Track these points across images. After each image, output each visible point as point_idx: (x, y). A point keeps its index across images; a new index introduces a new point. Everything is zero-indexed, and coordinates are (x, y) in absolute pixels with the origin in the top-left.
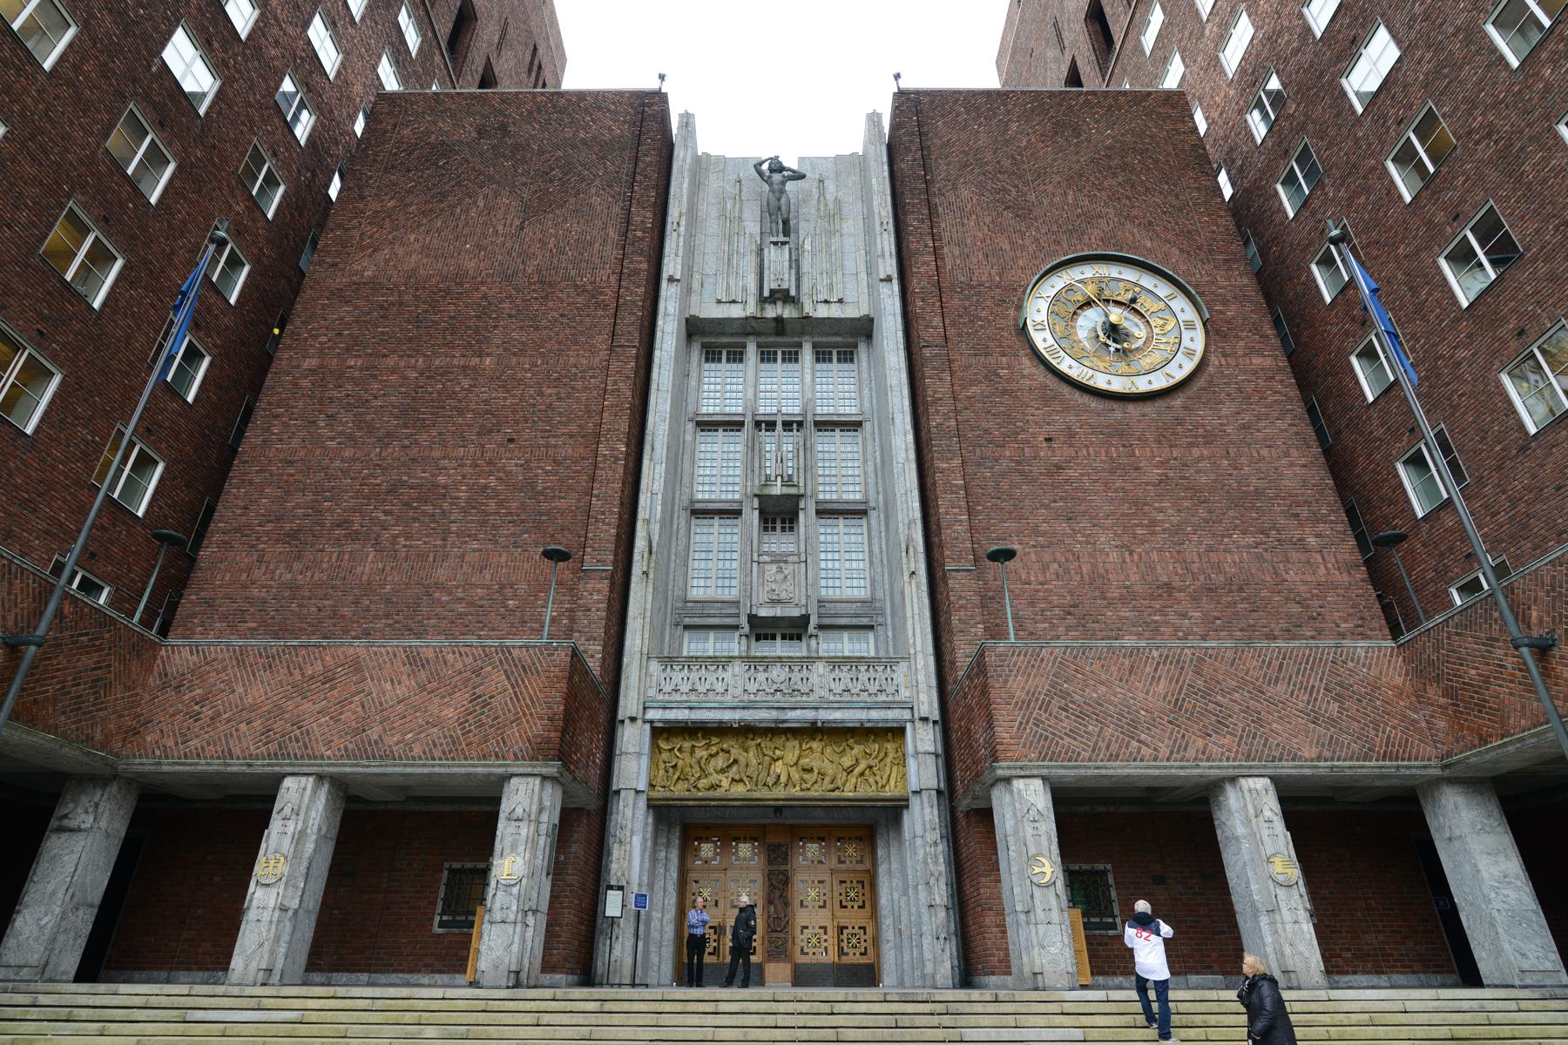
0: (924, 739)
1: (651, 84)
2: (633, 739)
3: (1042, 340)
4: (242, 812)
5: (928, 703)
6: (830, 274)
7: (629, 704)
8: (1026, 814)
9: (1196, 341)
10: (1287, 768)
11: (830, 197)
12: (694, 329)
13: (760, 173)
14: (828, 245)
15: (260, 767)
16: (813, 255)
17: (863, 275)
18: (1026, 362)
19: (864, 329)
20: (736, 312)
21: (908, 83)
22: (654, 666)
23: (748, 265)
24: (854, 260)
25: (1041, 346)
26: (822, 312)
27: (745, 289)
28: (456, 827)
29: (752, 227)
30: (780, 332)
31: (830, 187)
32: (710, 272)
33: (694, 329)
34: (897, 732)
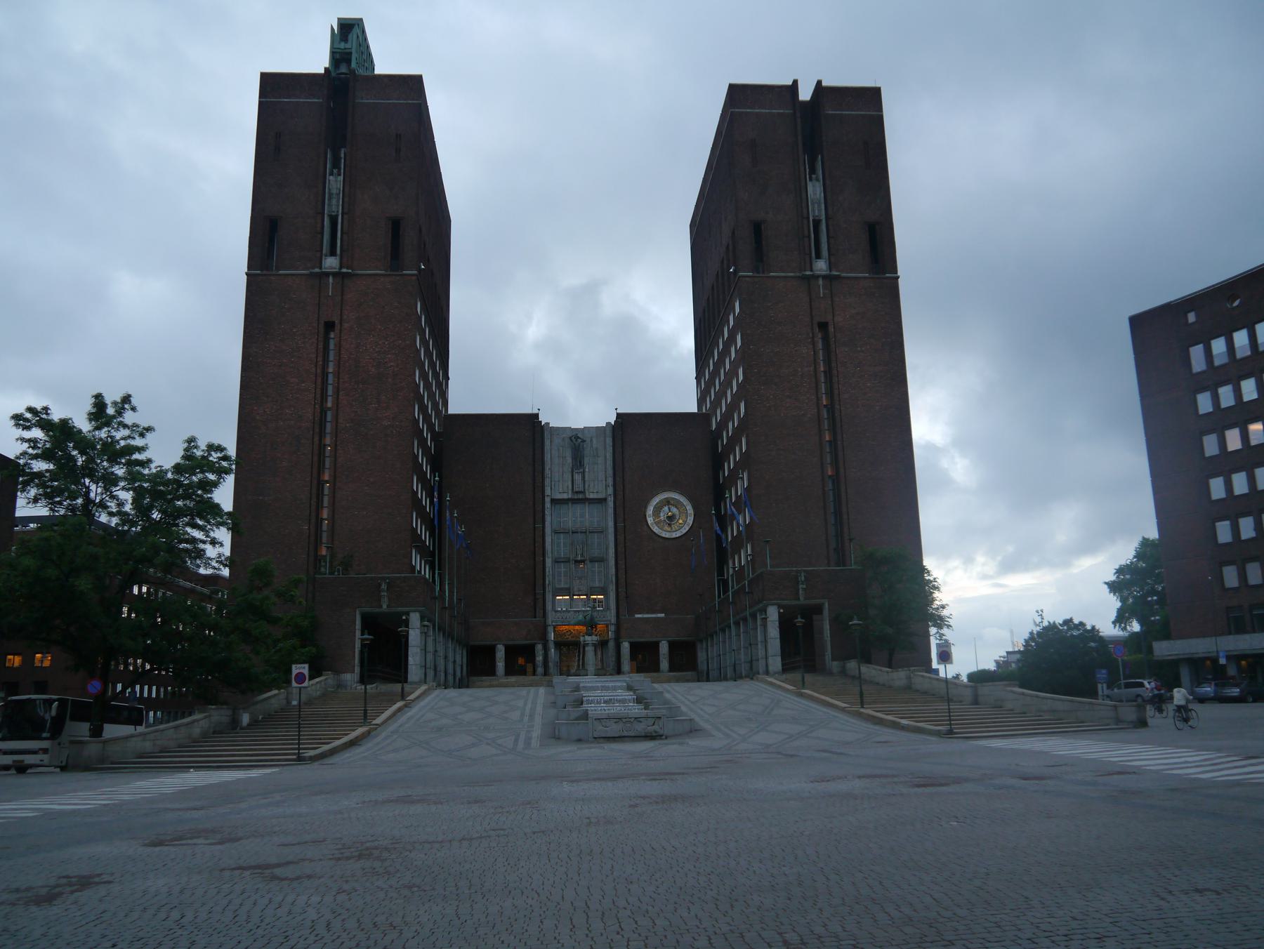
2: (550, 629)
3: (650, 520)
4: (491, 650)
5: (613, 620)
7: (549, 621)
8: (626, 646)
9: (690, 520)
19: (605, 500)
20: (565, 496)
23: (568, 476)
26: (592, 496)
28: (528, 651)
29: (569, 460)
30: (579, 499)
32: (558, 482)
33: (554, 501)
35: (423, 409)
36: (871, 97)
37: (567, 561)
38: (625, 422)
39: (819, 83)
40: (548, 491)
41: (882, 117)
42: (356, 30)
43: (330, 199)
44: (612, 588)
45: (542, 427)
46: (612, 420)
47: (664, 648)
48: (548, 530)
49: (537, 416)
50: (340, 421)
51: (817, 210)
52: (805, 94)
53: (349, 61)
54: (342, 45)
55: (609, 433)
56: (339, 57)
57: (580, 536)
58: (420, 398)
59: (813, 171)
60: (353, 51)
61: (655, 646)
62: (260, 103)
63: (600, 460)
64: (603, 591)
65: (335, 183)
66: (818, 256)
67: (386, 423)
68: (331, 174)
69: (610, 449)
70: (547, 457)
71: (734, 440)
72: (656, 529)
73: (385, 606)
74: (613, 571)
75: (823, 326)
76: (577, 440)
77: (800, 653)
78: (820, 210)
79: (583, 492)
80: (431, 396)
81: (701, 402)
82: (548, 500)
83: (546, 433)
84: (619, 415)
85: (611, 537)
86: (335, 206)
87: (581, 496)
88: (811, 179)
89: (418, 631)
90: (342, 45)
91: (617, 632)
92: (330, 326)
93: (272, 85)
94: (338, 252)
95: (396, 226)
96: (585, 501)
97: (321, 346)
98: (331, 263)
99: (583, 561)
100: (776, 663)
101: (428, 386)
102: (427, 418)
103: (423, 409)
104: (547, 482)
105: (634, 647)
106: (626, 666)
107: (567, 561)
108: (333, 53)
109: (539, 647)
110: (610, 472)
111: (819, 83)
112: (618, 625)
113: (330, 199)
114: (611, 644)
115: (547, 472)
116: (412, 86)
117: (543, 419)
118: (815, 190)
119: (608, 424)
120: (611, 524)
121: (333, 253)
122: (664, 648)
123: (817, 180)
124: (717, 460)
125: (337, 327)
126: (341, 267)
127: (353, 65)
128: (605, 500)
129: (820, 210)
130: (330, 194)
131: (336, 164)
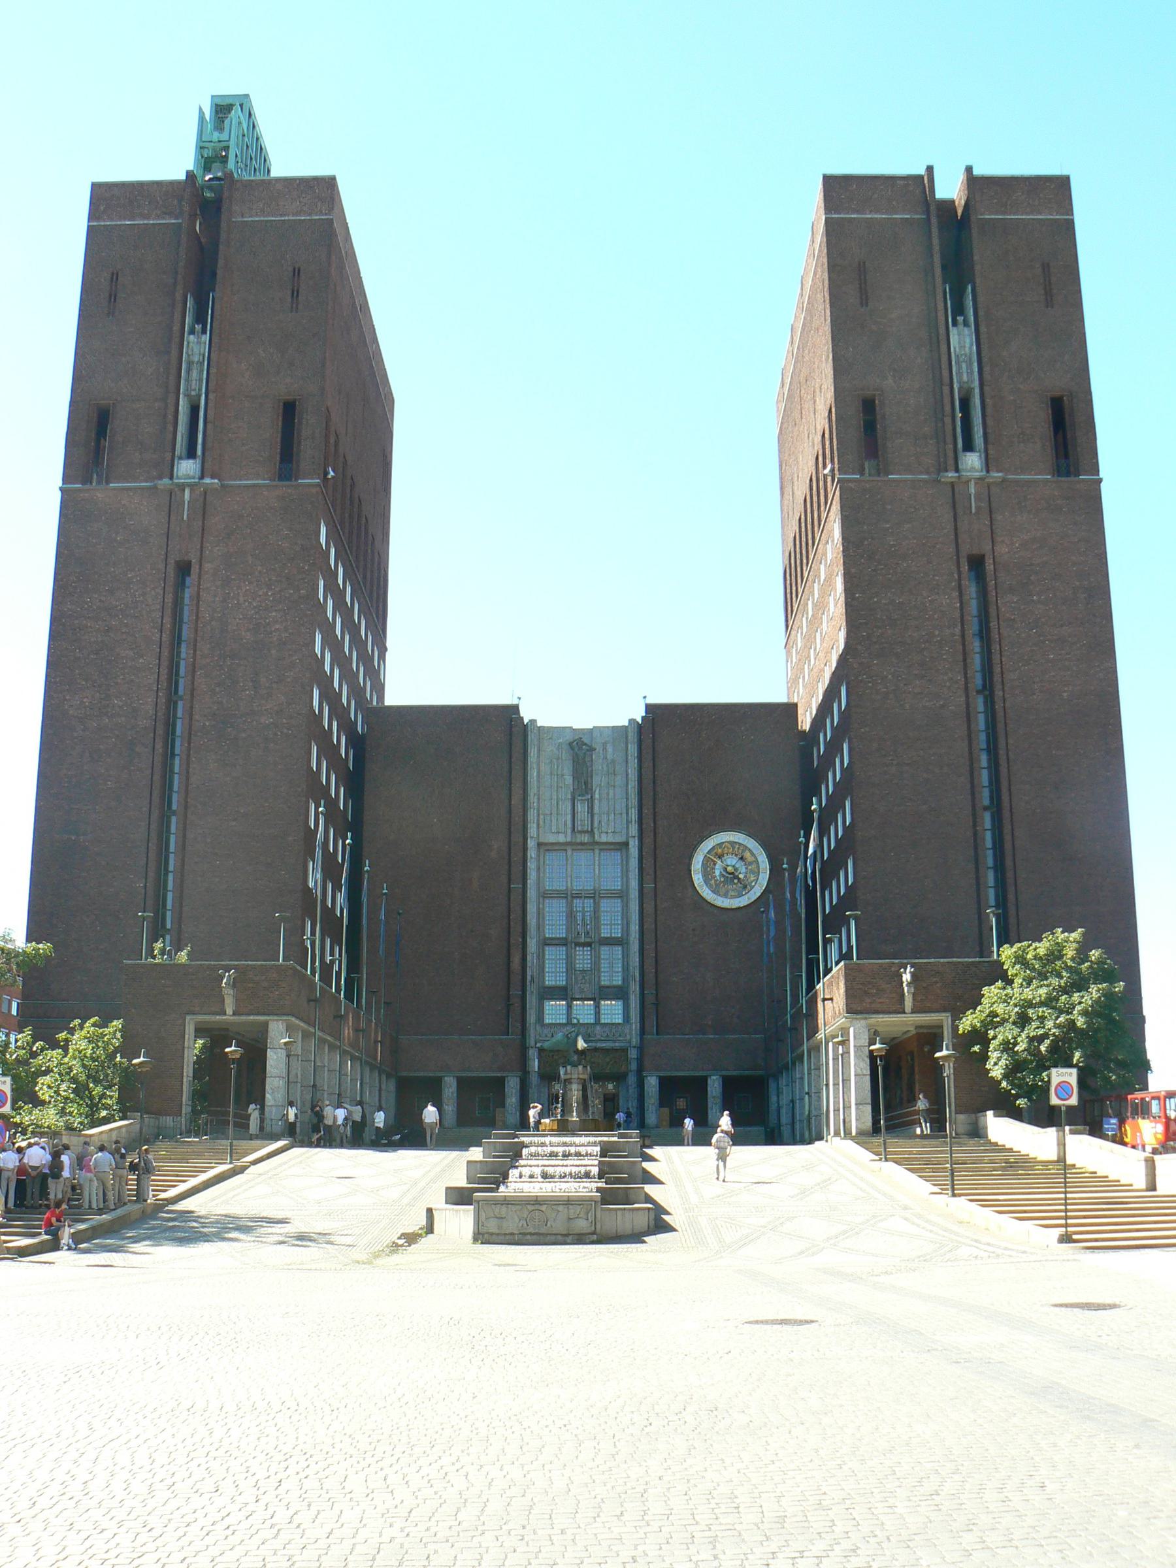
0: (633, 1054)
1: (515, 702)
2: (533, 1054)
3: (697, 879)
5: (635, 1041)
6: (608, 814)
7: (531, 1041)
8: (652, 1083)
10: (724, 1073)
11: (609, 757)
12: (539, 845)
13: (572, 749)
14: (608, 794)
15: (439, 1074)
16: (600, 800)
17: (624, 815)
18: (690, 890)
21: (650, 701)
22: (538, 1028)
24: (620, 806)
25: (696, 883)
26: (604, 839)
27: (565, 824)
29: (569, 780)
31: (610, 749)
34: (624, 1050)
35: (331, 697)
36: (1056, 190)
37: (563, 942)
38: (658, 715)
39: (969, 169)
40: (532, 830)
41: (1069, 228)
42: (235, 113)
43: (189, 370)
44: (634, 989)
45: (525, 726)
46: (639, 714)
47: (714, 1086)
48: (531, 894)
49: (515, 709)
50: (196, 717)
51: (966, 374)
52: (950, 188)
53: (225, 160)
54: (216, 136)
55: (632, 736)
56: (211, 156)
57: (588, 904)
58: (325, 683)
59: (959, 310)
60: (232, 144)
61: (700, 1084)
62: (91, 231)
63: (619, 780)
64: (619, 993)
65: (196, 345)
66: (969, 447)
67: (266, 720)
68: (192, 332)
69: (633, 763)
70: (533, 775)
71: (834, 747)
72: (706, 893)
73: (229, 1011)
74: (635, 960)
75: (977, 563)
76: (580, 748)
77: (914, 1098)
78: (970, 373)
79: (591, 832)
80: (349, 676)
81: (792, 684)
82: (531, 844)
83: (531, 738)
84: (649, 708)
85: (634, 906)
86: (194, 381)
87: (586, 838)
88: (955, 324)
89: (282, 1054)
90: (216, 136)
91: (640, 1060)
92: (184, 569)
93: (107, 200)
94: (199, 452)
95: (289, 410)
96: (592, 845)
97: (169, 598)
98: (187, 468)
99: (589, 944)
100: (858, 1116)
101: (340, 660)
102: (339, 712)
103: (331, 697)
104: (532, 815)
105: (664, 1082)
106: (651, 1118)
107: (563, 942)
108: (201, 148)
109: (512, 1085)
110: (634, 800)
111: (969, 169)
112: (641, 1048)
113: (189, 370)
114: (632, 1079)
115: (532, 798)
116: (323, 190)
117: (526, 715)
118: (961, 340)
119: (632, 721)
120: (634, 884)
121: (191, 454)
122: (714, 1086)
123: (966, 324)
124: (811, 782)
125: (195, 569)
126: (202, 477)
127: (231, 164)
128: (626, 844)
129: (970, 373)
130: (190, 363)
131: (200, 318)
